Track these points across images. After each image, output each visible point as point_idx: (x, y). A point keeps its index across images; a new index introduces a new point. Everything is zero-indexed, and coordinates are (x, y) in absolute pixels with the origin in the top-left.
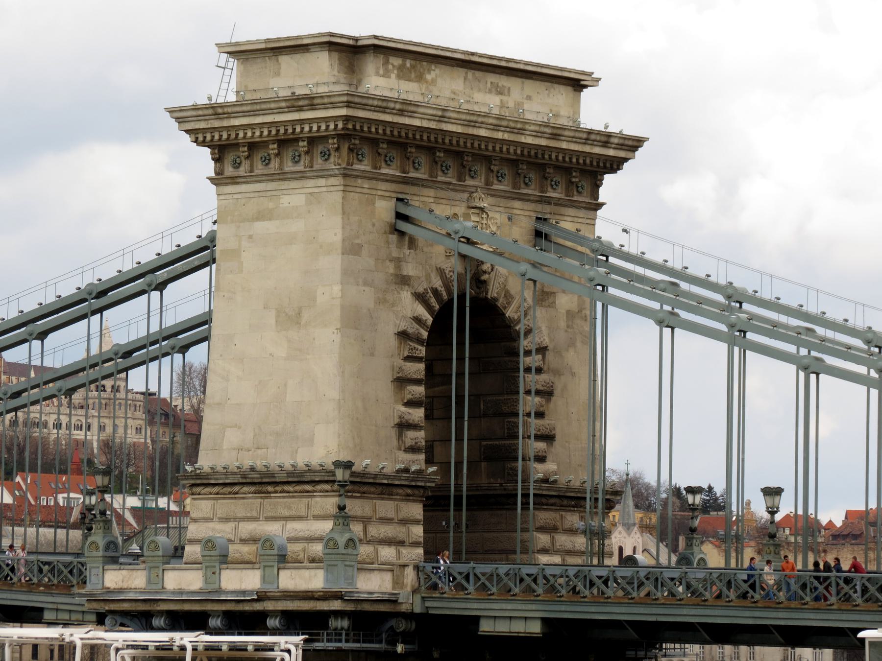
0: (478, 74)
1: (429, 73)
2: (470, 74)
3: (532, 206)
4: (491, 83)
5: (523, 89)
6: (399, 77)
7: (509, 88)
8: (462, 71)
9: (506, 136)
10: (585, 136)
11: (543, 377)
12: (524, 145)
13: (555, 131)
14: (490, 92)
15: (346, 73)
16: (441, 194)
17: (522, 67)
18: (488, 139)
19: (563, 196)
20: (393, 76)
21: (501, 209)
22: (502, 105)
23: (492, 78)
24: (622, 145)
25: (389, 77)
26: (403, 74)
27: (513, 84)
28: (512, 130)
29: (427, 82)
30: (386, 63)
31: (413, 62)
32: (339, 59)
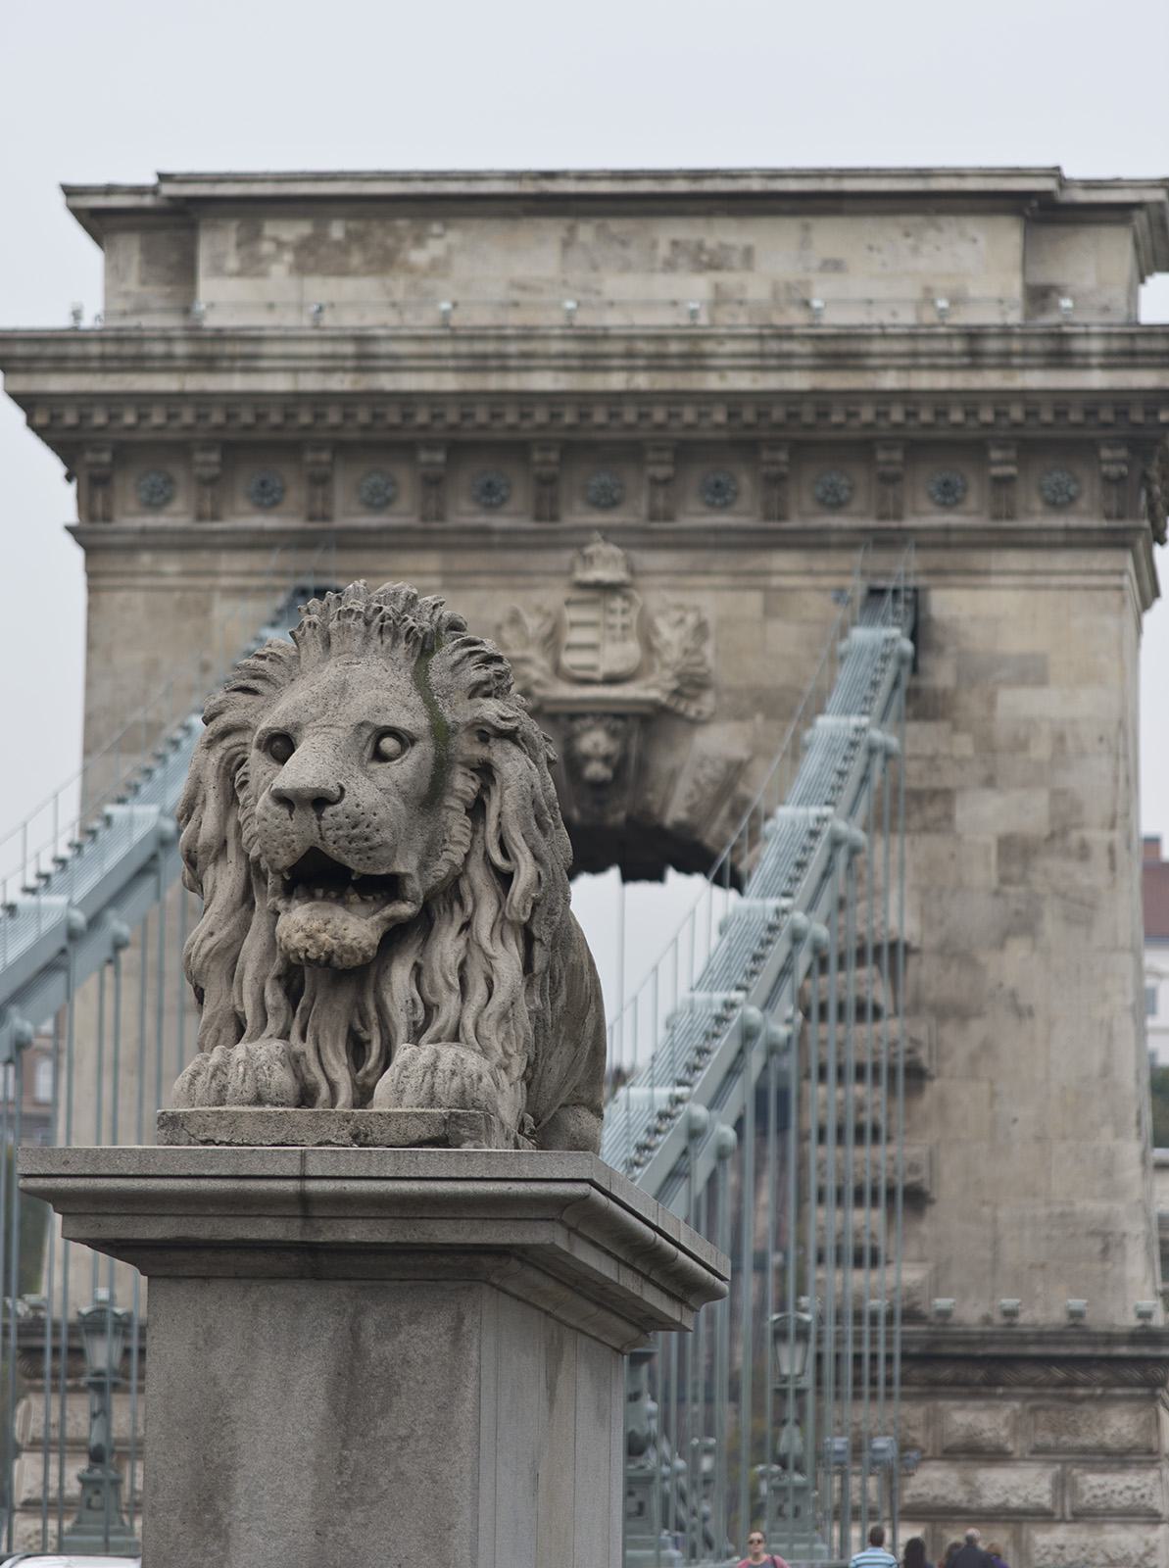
0: (616, 226)
1: (419, 241)
2: (586, 231)
3: (857, 558)
4: (675, 244)
5: (805, 244)
6: (300, 269)
7: (748, 253)
8: (553, 229)
9: (642, 381)
10: (958, 345)
11: (891, 1027)
12: (734, 400)
13: (829, 347)
14: (670, 266)
15: (170, 283)
17: (756, 185)
18: (584, 400)
19: (527, 523)
20: (279, 271)
21: (718, 580)
22: (720, 298)
23: (668, 232)
24: (1132, 353)
25: (263, 274)
26: (310, 259)
28: (658, 363)
29: (410, 269)
30: (251, 238)
31: (353, 225)
32: (145, 250)
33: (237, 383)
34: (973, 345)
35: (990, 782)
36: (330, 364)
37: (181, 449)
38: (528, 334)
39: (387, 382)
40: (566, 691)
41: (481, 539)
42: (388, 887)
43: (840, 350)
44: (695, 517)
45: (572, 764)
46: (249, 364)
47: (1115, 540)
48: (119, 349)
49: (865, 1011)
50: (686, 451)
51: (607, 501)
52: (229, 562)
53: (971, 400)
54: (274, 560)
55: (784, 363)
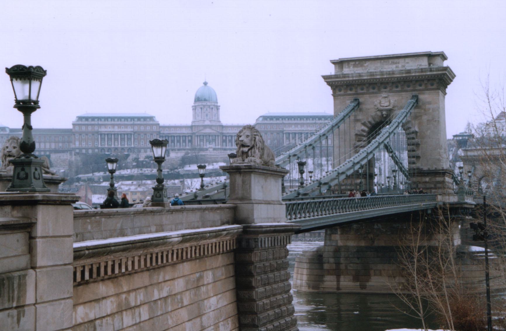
0: (386, 60)
1: (365, 63)
2: (382, 61)
3: (411, 93)
6: (353, 67)
8: (379, 61)
9: (388, 76)
11: (416, 140)
12: (397, 78)
14: (391, 64)
16: (372, 95)
20: (351, 67)
22: (397, 67)
23: (390, 61)
26: (355, 66)
27: (401, 61)
28: (389, 74)
30: (348, 64)
33: (347, 79)
34: (422, 70)
35: (425, 114)
36: (356, 77)
37: (342, 86)
38: (376, 72)
39: (362, 78)
40: (382, 108)
41: (373, 93)
42: (248, 146)
43: (409, 72)
44: (395, 89)
45: (382, 115)
46: (348, 77)
47: (438, 89)
48: (336, 76)
49: (413, 138)
50: (393, 83)
51: (385, 88)
52: (347, 97)
53: (422, 76)
54: (352, 96)
55: (403, 73)
